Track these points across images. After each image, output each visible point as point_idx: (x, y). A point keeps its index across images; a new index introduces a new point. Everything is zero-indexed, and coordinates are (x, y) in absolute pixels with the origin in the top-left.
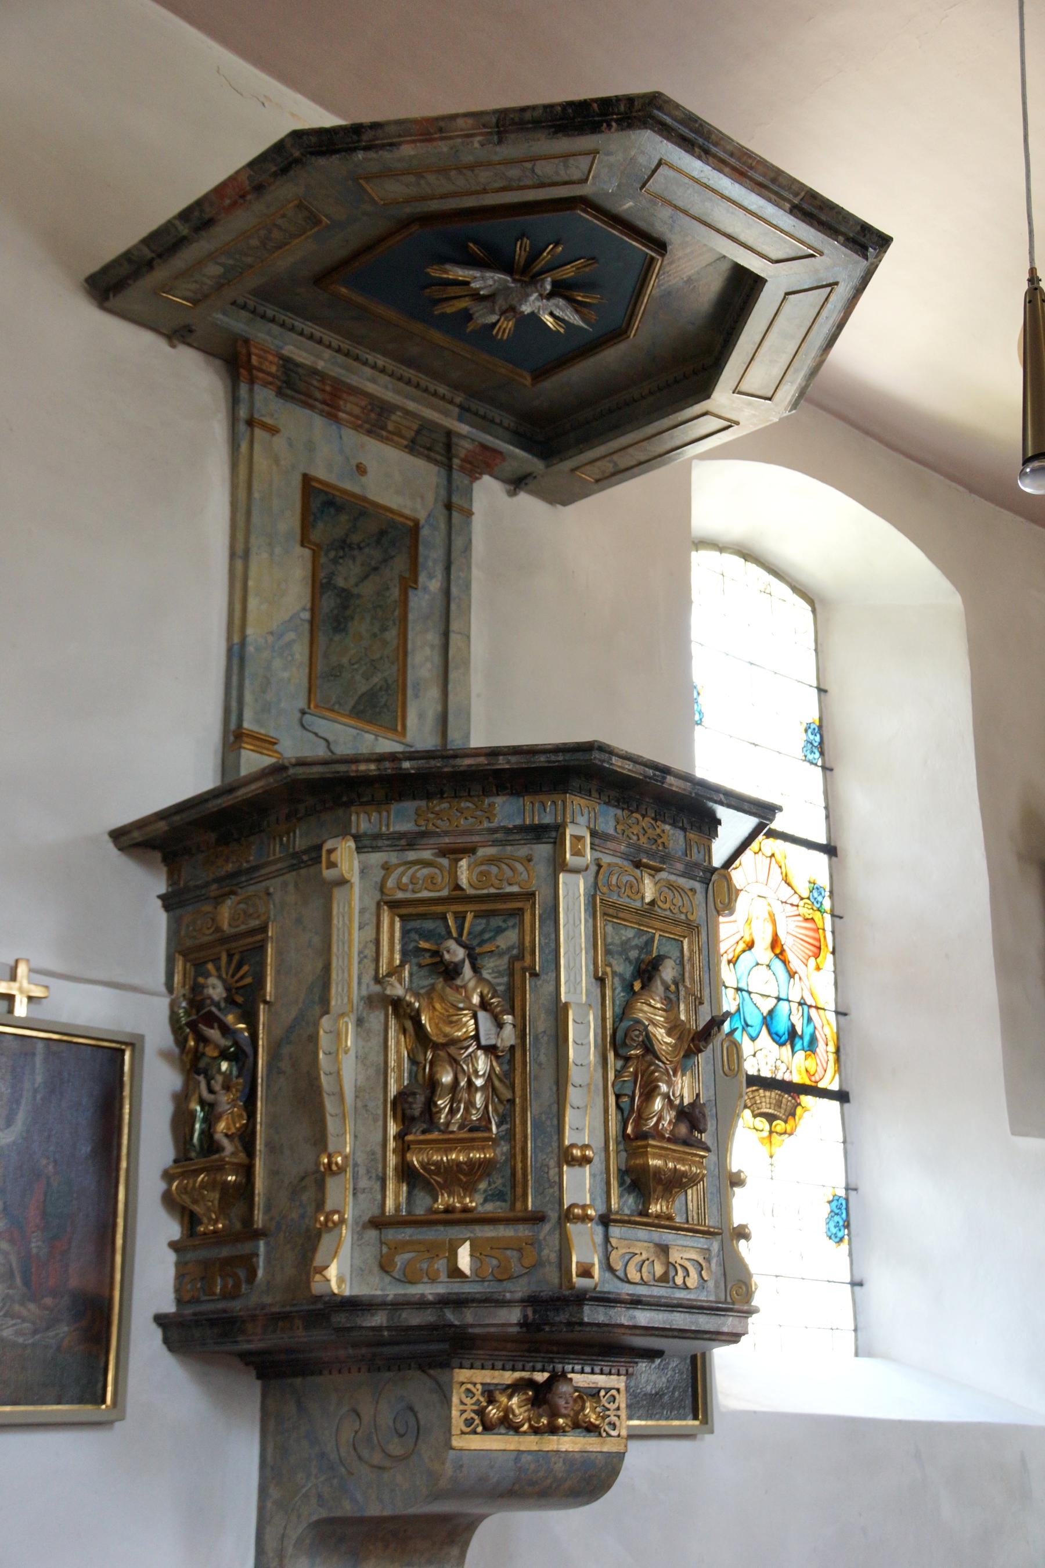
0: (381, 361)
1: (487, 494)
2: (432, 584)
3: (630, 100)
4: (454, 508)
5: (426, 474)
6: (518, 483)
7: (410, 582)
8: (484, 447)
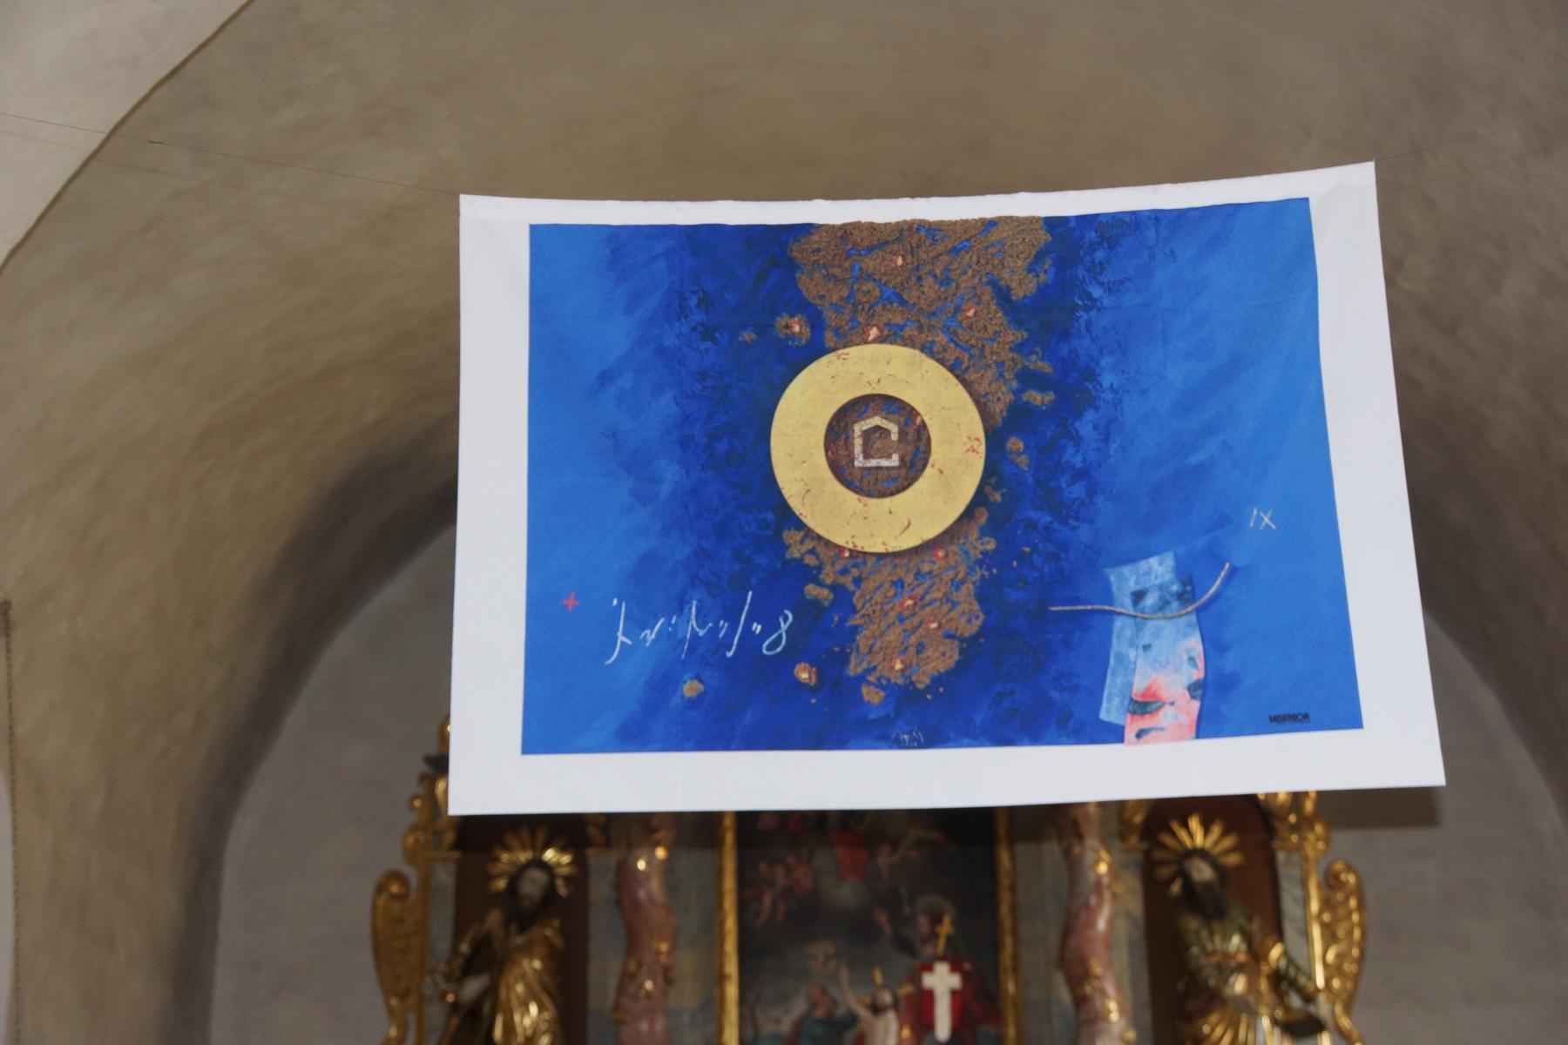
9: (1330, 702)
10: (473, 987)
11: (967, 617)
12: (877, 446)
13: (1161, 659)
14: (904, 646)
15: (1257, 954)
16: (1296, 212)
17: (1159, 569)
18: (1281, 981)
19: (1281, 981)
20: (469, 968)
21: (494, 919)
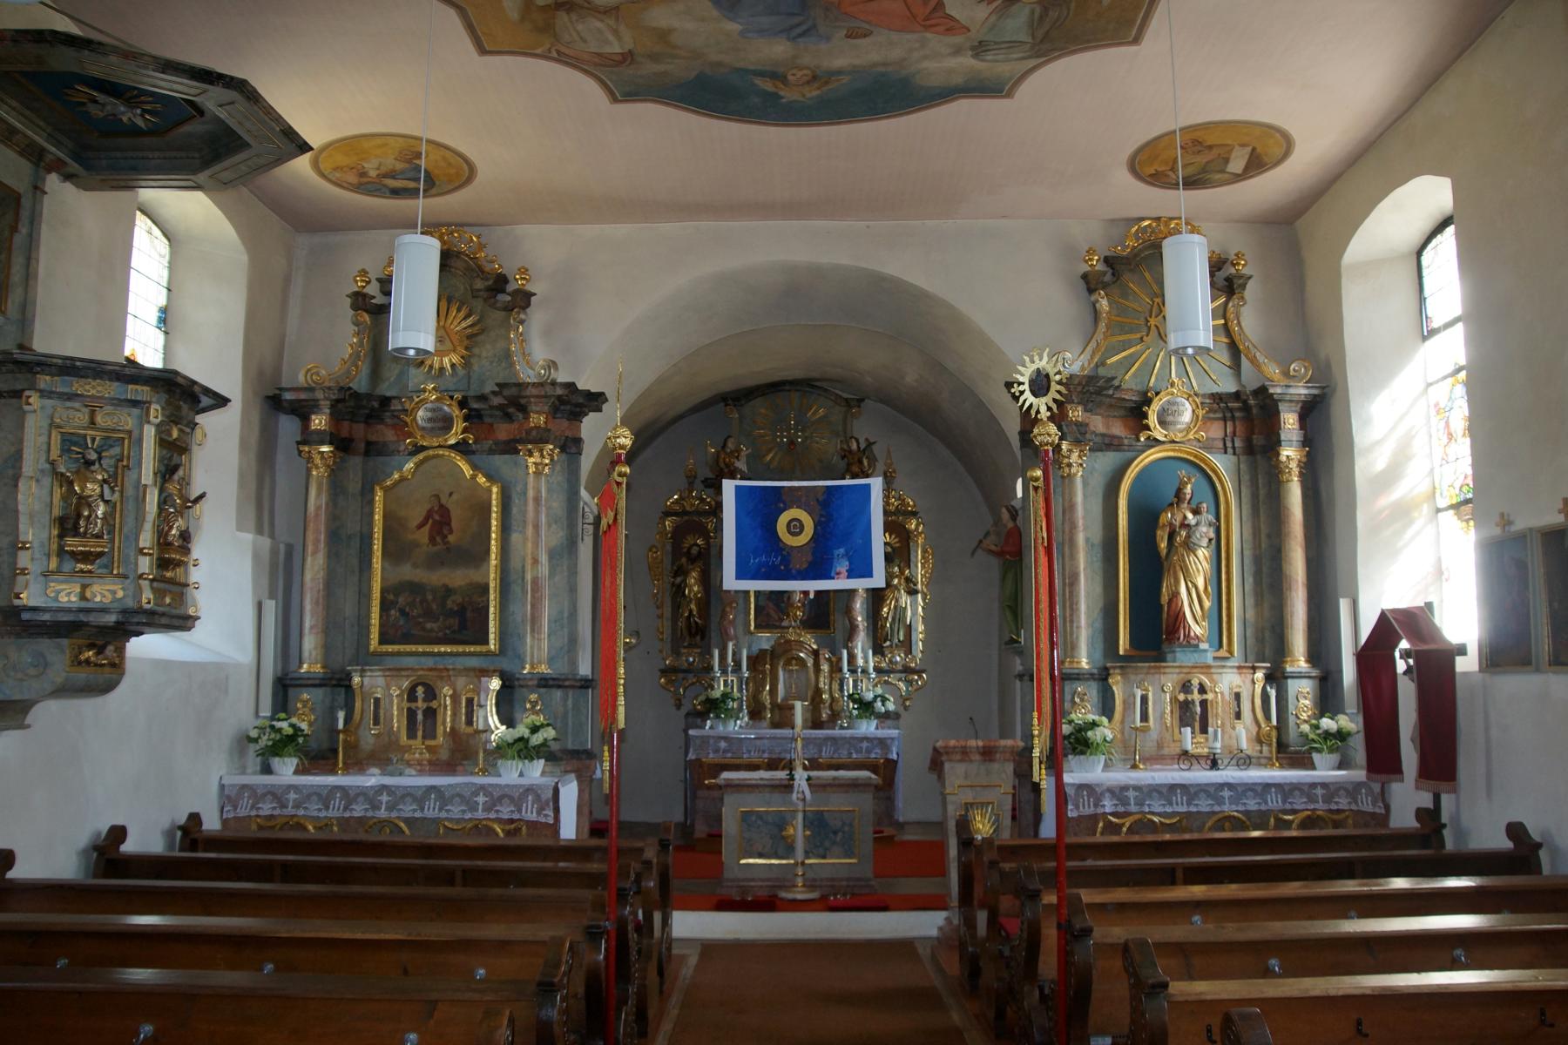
0: (14, 104)
1: (53, 181)
2: (24, 230)
3: (232, 78)
4: (38, 189)
5: (25, 166)
6: (68, 177)
7: (14, 229)
8: (59, 159)
9: (868, 573)
10: (679, 580)
11: (810, 558)
12: (795, 527)
13: (842, 566)
14: (799, 563)
15: (902, 572)
16: (868, 486)
17: (842, 551)
18: (908, 580)
19: (908, 580)
20: (676, 575)
21: (684, 560)
